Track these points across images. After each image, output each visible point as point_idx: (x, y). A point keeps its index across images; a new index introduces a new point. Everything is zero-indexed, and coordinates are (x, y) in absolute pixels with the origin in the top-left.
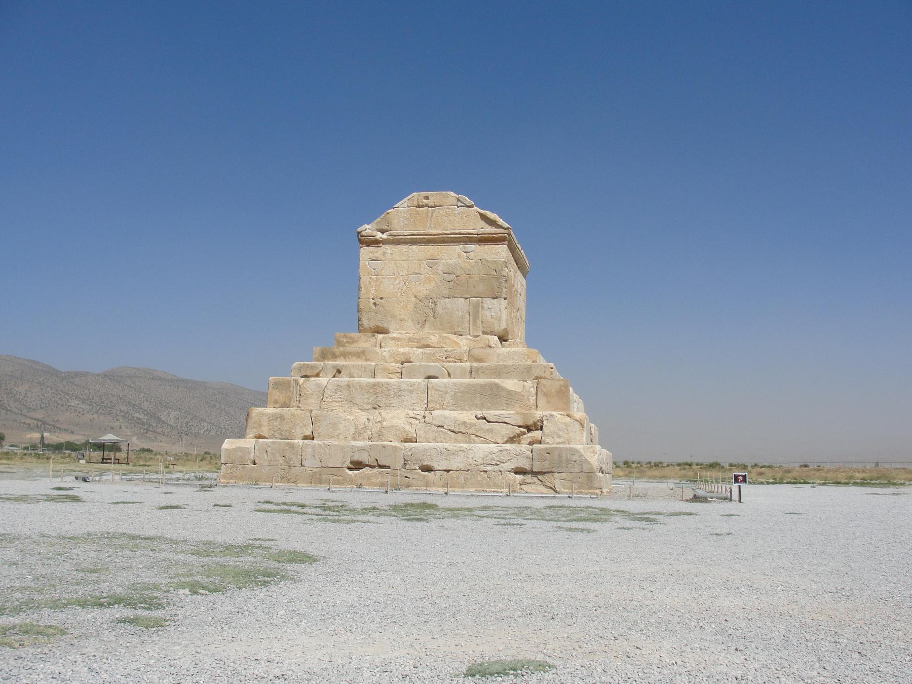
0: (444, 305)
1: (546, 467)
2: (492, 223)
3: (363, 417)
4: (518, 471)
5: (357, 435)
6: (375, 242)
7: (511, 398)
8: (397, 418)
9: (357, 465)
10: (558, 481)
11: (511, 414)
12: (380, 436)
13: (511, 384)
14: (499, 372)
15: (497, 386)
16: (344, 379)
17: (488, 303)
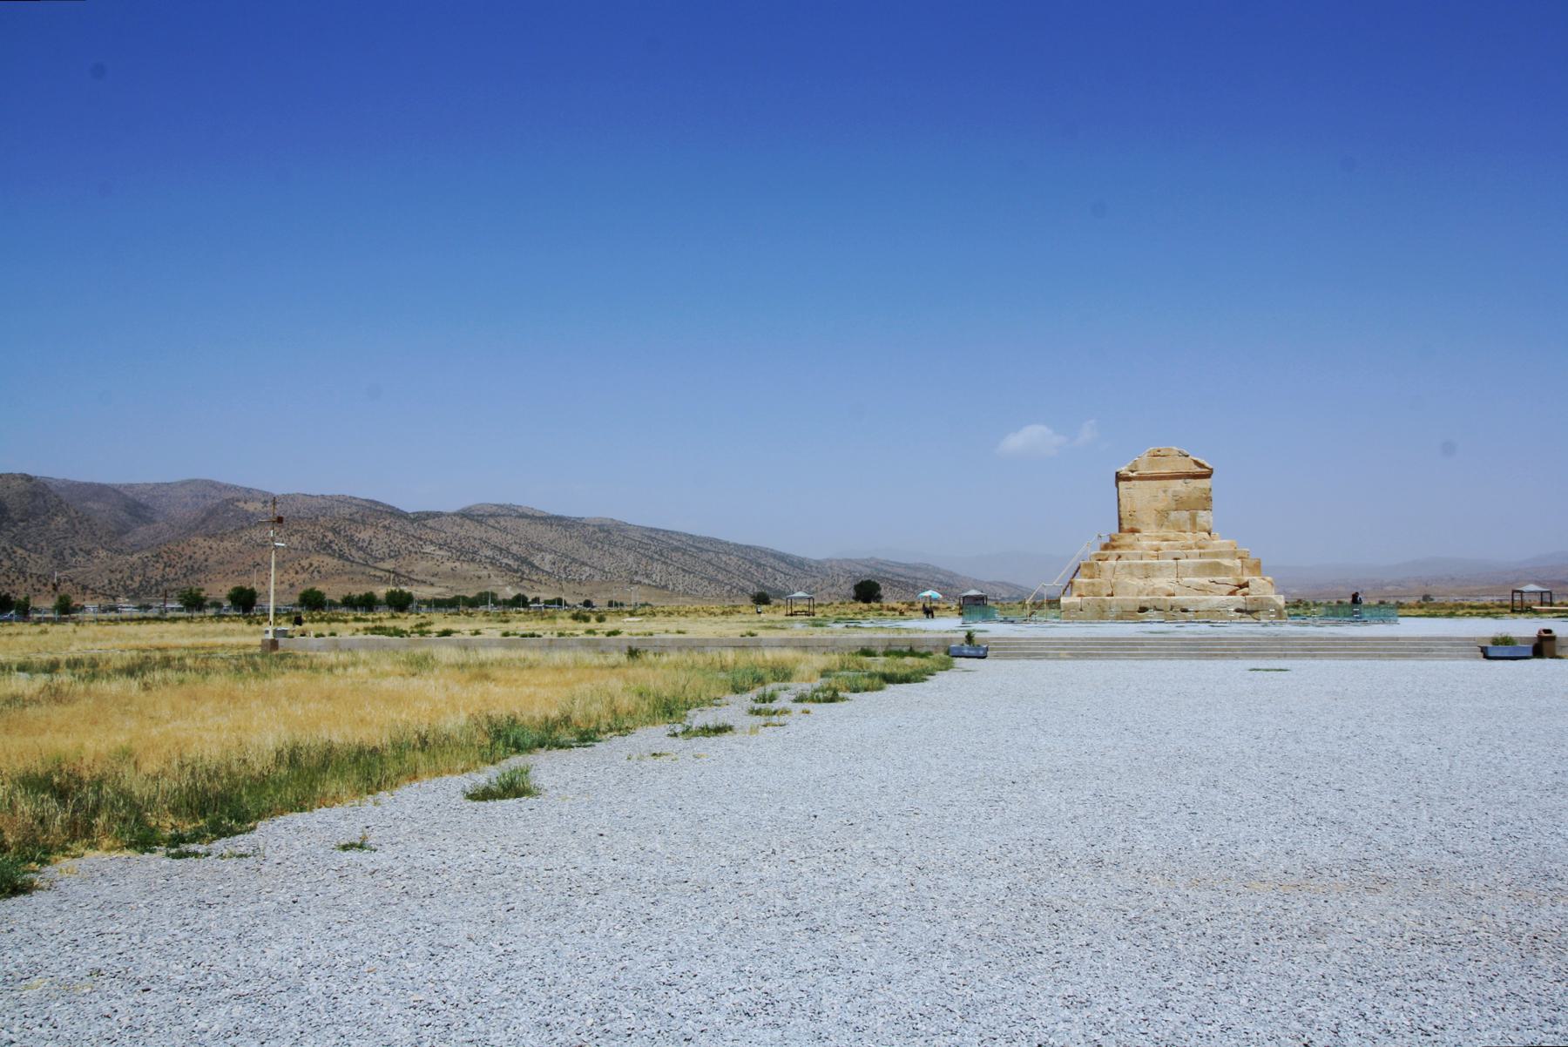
0: (1173, 515)
1: (1254, 607)
2: (1201, 466)
3: (1141, 583)
4: (1238, 611)
5: (1140, 593)
6: (1129, 479)
7: (1228, 570)
8: (1162, 582)
9: (1143, 610)
10: (1261, 615)
11: (1231, 579)
12: (1153, 593)
13: (1226, 562)
14: (1216, 555)
15: (1219, 564)
16: (1123, 562)
17: (1201, 513)
